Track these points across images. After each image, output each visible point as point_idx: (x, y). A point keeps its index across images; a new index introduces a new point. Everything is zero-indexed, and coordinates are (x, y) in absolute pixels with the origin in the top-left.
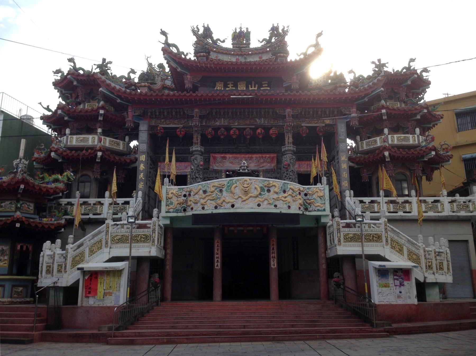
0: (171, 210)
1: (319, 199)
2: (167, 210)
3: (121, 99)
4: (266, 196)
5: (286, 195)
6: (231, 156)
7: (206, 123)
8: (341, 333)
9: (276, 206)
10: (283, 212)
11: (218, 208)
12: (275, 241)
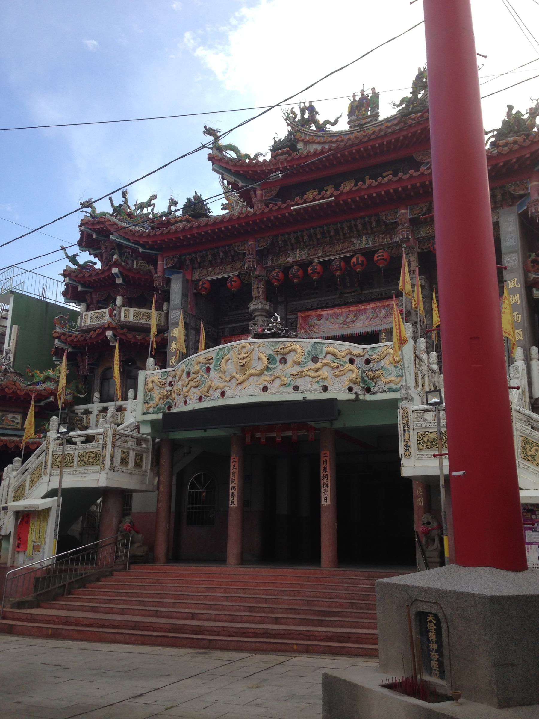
0: (151, 410)
1: (392, 368)
2: (145, 411)
3: (143, 246)
4: (279, 372)
5: (318, 365)
6: (331, 312)
7: (272, 262)
8: (357, 642)
9: (296, 388)
10: (308, 398)
11: (203, 399)
12: (328, 454)
